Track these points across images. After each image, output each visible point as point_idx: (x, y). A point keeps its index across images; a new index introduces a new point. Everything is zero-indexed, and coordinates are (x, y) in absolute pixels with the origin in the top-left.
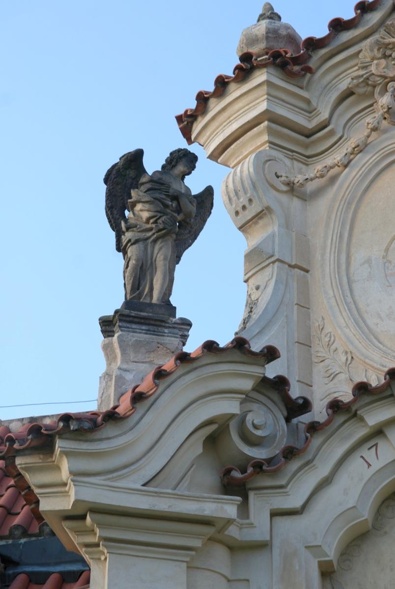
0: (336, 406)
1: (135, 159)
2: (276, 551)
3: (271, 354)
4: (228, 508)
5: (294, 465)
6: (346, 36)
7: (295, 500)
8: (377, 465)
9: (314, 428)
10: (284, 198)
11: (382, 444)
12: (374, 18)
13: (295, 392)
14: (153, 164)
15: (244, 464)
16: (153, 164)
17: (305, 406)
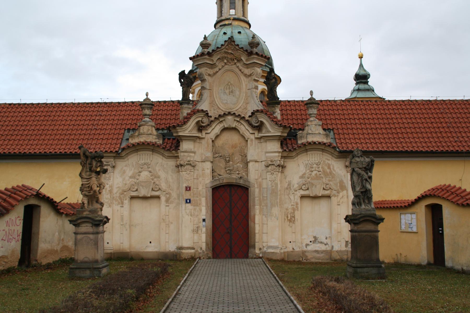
0: (215, 118)
1: (183, 72)
2: (206, 139)
3: (207, 111)
4: (199, 135)
5: (209, 127)
6: (219, 50)
7: (209, 132)
8: (221, 126)
9: (212, 121)
10: (208, 77)
11: (222, 123)
12: (223, 47)
13: (209, 115)
14: (186, 72)
15: (202, 126)
16: (186, 72)
17: (211, 117)
